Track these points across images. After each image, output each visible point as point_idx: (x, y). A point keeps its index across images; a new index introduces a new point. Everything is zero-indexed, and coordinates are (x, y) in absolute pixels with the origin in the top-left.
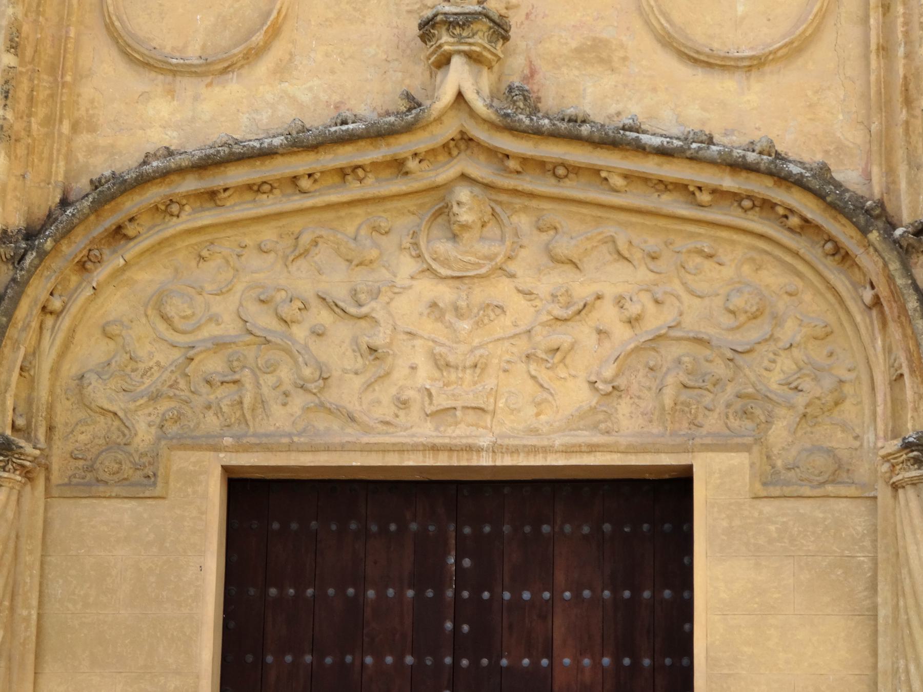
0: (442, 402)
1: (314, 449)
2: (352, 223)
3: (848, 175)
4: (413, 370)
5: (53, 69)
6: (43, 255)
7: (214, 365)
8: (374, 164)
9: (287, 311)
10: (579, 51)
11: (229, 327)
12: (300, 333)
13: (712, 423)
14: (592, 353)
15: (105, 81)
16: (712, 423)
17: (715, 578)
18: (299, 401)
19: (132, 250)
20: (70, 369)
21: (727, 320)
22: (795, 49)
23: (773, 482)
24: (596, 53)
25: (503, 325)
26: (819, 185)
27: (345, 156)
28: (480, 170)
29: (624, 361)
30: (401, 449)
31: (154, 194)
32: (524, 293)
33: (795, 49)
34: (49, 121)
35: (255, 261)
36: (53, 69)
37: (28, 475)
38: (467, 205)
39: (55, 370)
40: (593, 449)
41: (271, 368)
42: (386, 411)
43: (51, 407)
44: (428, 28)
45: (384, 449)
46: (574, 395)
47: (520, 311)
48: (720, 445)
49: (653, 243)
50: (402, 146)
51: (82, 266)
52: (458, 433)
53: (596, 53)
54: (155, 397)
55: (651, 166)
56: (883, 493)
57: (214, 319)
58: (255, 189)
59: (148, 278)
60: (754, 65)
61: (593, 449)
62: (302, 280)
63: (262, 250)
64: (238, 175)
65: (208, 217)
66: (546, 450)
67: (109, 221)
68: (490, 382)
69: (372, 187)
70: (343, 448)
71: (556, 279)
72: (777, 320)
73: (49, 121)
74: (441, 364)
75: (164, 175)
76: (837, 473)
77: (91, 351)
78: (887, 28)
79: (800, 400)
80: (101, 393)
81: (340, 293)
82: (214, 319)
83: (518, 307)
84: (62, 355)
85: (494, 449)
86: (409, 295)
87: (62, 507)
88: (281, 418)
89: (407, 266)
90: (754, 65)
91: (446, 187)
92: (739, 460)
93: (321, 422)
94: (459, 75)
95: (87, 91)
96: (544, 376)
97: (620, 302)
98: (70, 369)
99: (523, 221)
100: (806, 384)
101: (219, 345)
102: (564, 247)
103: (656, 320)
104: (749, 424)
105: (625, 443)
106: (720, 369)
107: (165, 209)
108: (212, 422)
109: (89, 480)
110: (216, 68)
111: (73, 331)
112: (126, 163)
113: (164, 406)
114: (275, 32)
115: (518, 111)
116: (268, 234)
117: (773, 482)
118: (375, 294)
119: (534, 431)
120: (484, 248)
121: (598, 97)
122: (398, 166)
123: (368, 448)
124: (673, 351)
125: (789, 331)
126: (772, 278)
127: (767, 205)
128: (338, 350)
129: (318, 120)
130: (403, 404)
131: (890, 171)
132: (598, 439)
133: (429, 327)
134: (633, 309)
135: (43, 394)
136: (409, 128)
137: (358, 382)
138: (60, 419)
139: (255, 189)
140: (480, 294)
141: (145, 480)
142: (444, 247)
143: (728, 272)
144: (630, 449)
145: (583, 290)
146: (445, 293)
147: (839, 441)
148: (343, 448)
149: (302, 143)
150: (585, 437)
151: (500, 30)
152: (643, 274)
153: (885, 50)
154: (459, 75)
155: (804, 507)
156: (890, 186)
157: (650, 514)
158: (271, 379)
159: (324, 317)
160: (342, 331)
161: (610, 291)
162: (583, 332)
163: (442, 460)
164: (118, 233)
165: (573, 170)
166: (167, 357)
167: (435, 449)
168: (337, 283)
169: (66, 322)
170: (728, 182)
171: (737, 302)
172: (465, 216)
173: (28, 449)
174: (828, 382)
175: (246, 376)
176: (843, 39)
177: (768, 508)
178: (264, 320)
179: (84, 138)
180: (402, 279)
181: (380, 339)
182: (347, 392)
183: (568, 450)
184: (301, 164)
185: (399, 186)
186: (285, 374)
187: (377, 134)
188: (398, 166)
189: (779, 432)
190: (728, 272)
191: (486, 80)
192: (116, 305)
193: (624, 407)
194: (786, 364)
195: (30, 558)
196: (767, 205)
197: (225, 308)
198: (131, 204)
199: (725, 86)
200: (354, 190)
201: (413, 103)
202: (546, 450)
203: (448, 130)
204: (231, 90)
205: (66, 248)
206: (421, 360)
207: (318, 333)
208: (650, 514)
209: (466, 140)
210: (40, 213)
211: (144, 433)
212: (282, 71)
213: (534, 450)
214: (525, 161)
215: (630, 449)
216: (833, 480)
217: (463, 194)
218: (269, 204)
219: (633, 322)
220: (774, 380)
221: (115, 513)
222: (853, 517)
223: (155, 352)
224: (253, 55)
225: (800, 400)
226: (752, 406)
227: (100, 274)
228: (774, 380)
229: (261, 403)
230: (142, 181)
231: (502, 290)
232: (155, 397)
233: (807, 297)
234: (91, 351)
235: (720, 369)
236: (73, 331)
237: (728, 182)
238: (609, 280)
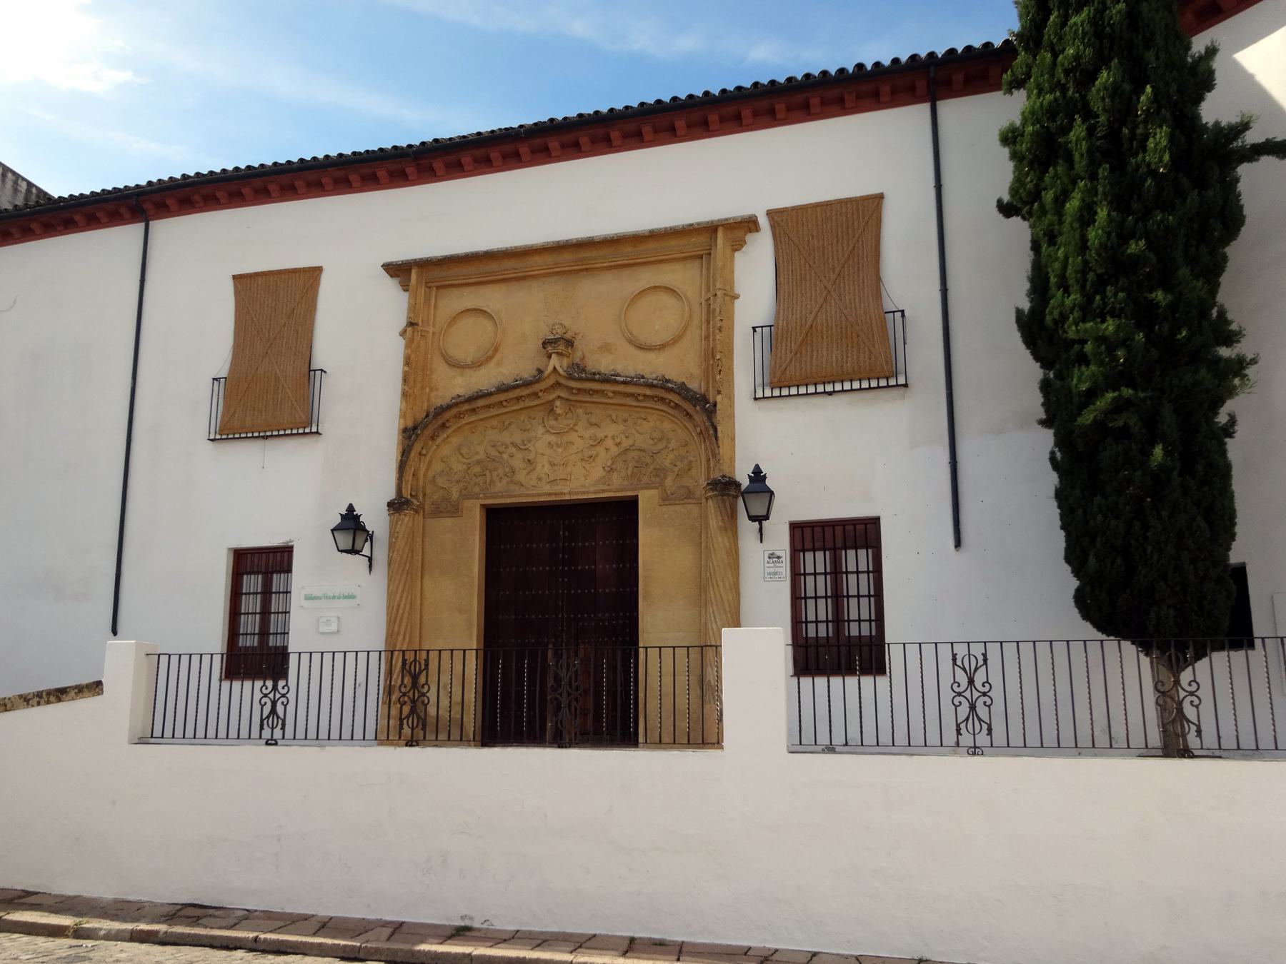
0: (552, 478)
1: (510, 496)
2: (523, 417)
3: (693, 385)
4: (543, 467)
5: (423, 370)
6: (418, 436)
7: (477, 469)
8: (528, 395)
9: (501, 449)
10: (600, 348)
11: (482, 456)
12: (505, 456)
13: (645, 479)
14: (603, 457)
15: (441, 372)
16: (645, 479)
17: (647, 536)
18: (505, 480)
19: (450, 431)
20: (431, 474)
21: (651, 442)
22: (675, 341)
23: (666, 499)
24: (606, 348)
25: (574, 449)
26: (682, 389)
27: (517, 393)
28: (564, 394)
29: (614, 460)
30: (539, 495)
31: (455, 411)
32: (579, 440)
33: (675, 341)
34: (422, 389)
35: (490, 432)
36: (423, 370)
37: (416, 512)
38: (559, 407)
39: (425, 475)
40: (604, 491)
41: (496, 469)
42: (533, 482)
43: (424, 488)
44: (545, 344)
45: (533, 495)
46: (598, 472)
47: (579, 443)
48: (647, 487)
49: (625, 415)
50: (537, 387)
51: (433, 438)
52: (559, 488)
53: (606, 348)
54: (458, 482)
55: (621, 388)
56: (703, 500)
57: (477, 453)
58: (488, 407)
59: (455, 440)
60: (661, 347)
61: (604, 491)
62: (506, 438)
63: (493, 428)
64: (481, 403)
65: (473, 418)
66: (587, 493)
67: (440, 422)
68: (569, 469)
69: (528, 403)
70: (520, 496)
71: (592, 431)
72: (668, 441)
73: (422, 389)
74: (552, 465)
75: (456, 404)
76: (689, 495)
77: (438, 467)
78: (708, 329)
79: (676, 469)
80: (440, 481)
81: (519, 442)
82: (477, 453)
83: (579, 443)
84: (427, 470)
85: (570, 493)
86: (542, 439)
87: (428, 521)
88: (499, 486)
89: (541, 430)
90: (661, 347)
91: (553, 401)
92: (654, 492)
93: (512, 487)
94: (555, 361)
95: (435, 377)
96: (587, 466)
97: (613, 438)
98: (431, 474)
99: (580, 411)
100: (678, 463)
101: (479, 462)
102: (594, 420)
103: (626, 444)
104: (658, 479)
105: (615, 488)
106: (649, 460)
107: (459, 416)
108: (477, 489)
109: (437, 513)
110: (477, 365)
111: (430, 461)
112: (447, 401)
113: (461, 484)
114: (496, 350)
115: (579, 372)
116: (494, 422)
117: (666, 499)
118: (529, 441)
119: (583, 486)
120: (566, 422)
121: (603, 363)
122: (535, 395)
123: (528, 495)
124: (632, 454)
125: (673, 444)
126: (667, 425)
127: (662, 399)
128: (517, 462)
129: (509, 381)
130: (540, 479)
131: (708, 383)
132: (605, 488)
133: (548, 452)
134: (618, 440)
135: (421, 483)
136: (538, 381)
137: (525, 472)
138: (428, 491)
139: (488, 407)
140: (566, 438)
141: (452, 509)
142: (552, 422)
143: (652, 424)
144: (617, 491)
145: (600, 434)
146: (553, 439)
147: (689, 482)
148: (520, 496)
149: (503, 389)
150: (601, 487)
151: (570, 343)
152: (622, 427)
153: (707, 338)
154: (555, 361)
155: (677, 508)
156: (707, 390)
157: (621, 515)
158: (495, 474)
159: (513, 450)
160: (519, 455)
161: (610, 435)
162: (601, 450)
163: (553, 498)
164: (443, 426)
165: (596, 392)
166: (461, 467)
167: (550, 494)
168: (518, 437)
169: (428, 458)
170: (648, 392)
171: (654, 435)
172: (559, 411)
173: (416, 502)
174: (686, 462)
175: (487, 472)
176: (694, 334)
177: (665, 509)
178: (493, 453)
179: (433, 394)
180: (539, 435)
181: (531, 456)
182: (521, 476)
183: (595, 492)
184: (502, 397)
185: (537, 402)
186: (500, 471)
187: (527, 384)
188: (535, 395)
189: (669, 482)
190: (652, 424)
191: (565, 362)
192: (445, 451)
193: (615, 475)
194: (671, 456)
195: (419, 539)
196: (662, 399)
197: (480, 449)
198: (447, 415)
199: (651, 356)
200: (521, 405)
201: (540, 371)
202: (587, 493)
203: (551, 381)
204: (483, 372)
205: (426, 432)
206: (546, 463)
207: (511, 456)
208: (621, 515)
209: (558, 385)
210: (419, 419)
211: (455, 495)
212: (499, 364)
213: (584, 493)
214: (579, 390)
215: (617, 491)
216: (687, 497)
217: (558, 403)
218: (494, 412)
219: (618, 444)
220: (667, 463)
221: (448, 522)
222: (694, 510)
223: (459, 467)
224: (489, 359)
225: (676, 469)
226: (660, 472)
227: (439, 441)
228: (667, 463)
229: (492, 481)
230: (449, 407)
231: (573, 437)
232: (458, 482)
233: (679, 431)
234: (438, 467)
235: (649, 460)
236: (430, 461)
237: (648, 392)
238: (610, 430)
